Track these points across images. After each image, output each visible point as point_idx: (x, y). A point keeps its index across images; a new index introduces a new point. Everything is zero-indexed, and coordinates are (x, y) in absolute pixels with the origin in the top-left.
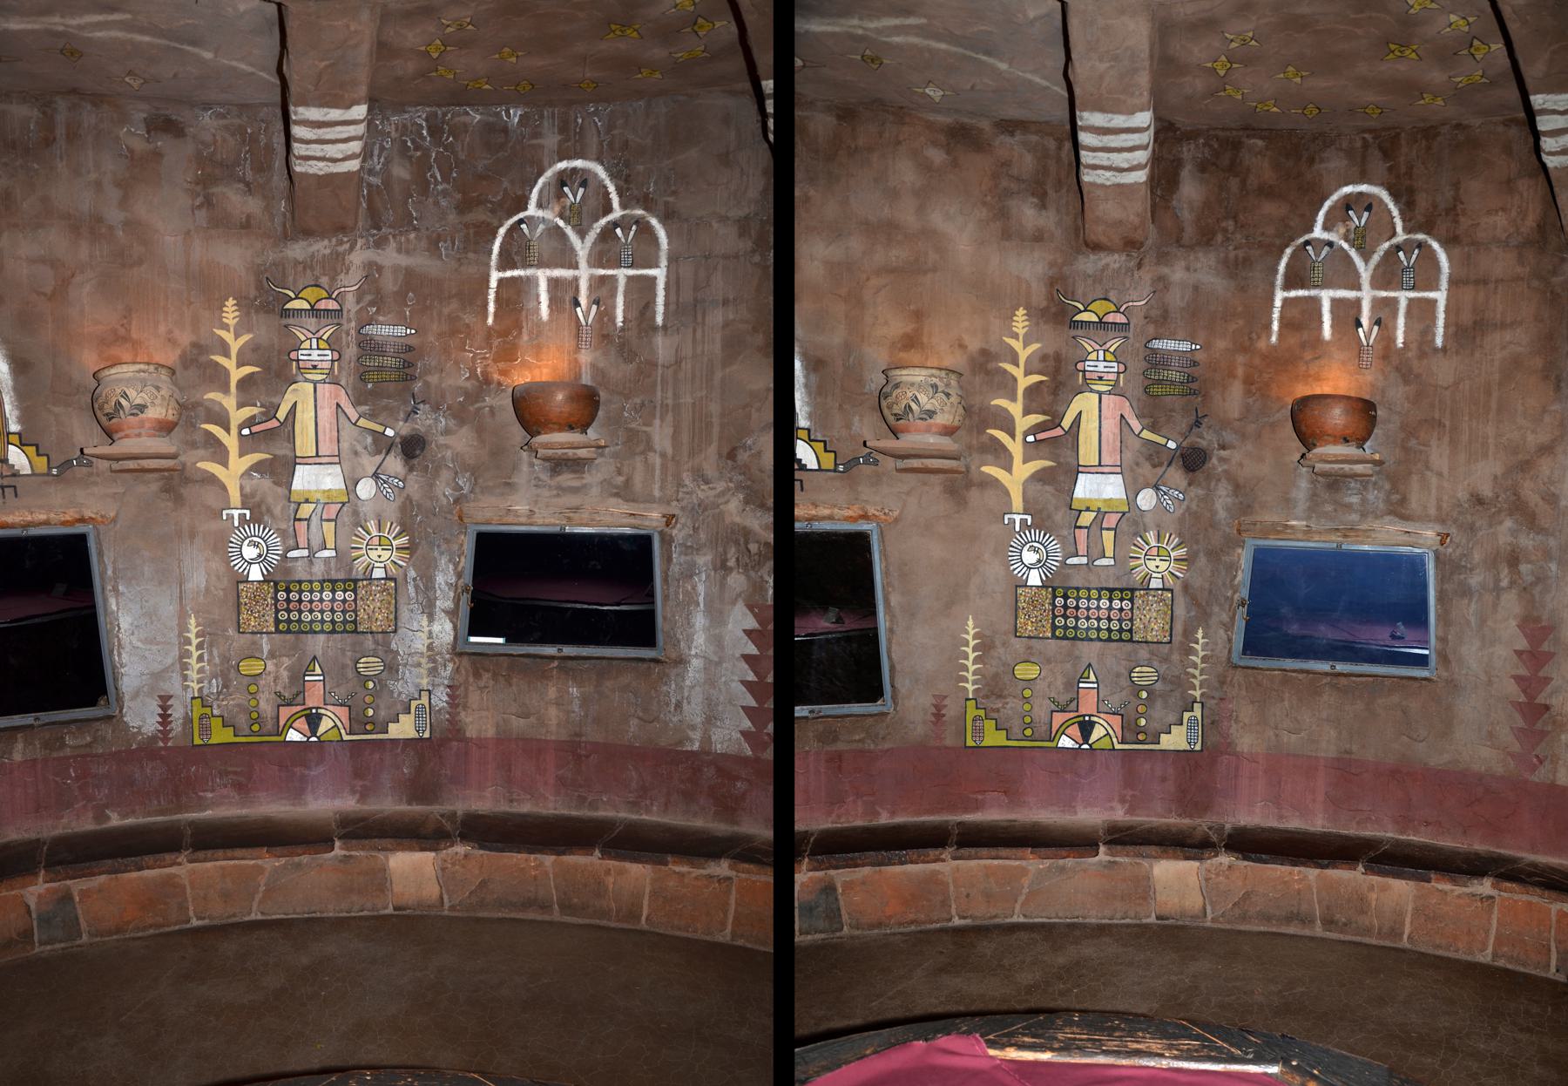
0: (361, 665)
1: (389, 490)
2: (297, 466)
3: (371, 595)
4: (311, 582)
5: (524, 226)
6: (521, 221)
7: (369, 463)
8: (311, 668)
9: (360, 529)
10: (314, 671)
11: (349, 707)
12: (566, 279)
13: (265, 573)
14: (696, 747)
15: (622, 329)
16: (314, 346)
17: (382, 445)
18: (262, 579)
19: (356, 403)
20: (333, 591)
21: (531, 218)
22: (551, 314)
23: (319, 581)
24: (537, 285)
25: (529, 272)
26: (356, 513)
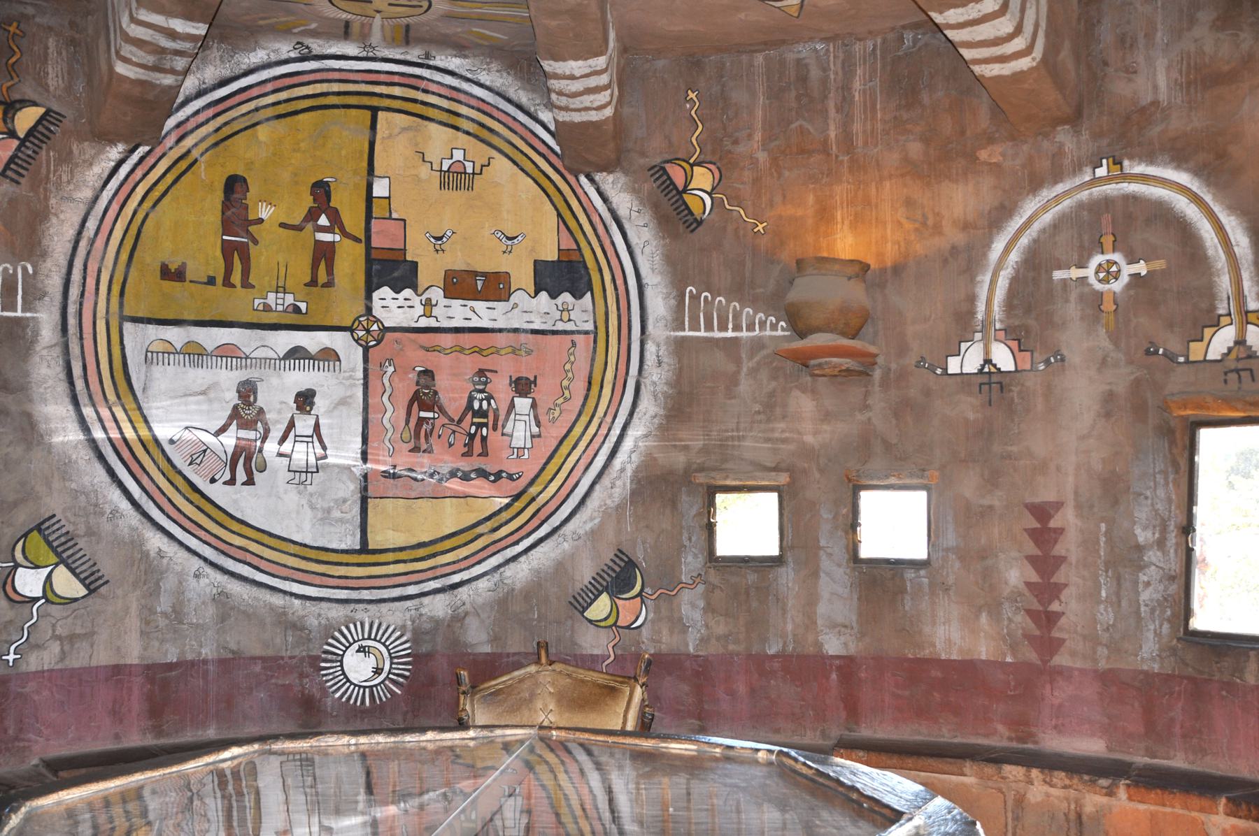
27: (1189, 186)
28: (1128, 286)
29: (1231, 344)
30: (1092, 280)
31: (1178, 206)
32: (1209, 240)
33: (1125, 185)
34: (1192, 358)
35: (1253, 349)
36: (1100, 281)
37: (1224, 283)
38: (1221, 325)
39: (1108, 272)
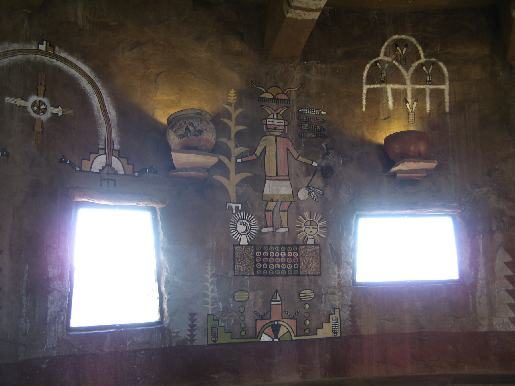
0: (302, 295)
1: (315, 196)
2: (267, 181)
3: (307, 254)
4: (274, 246)
5: (378, 64)
6: (377, 62)
7: (305, 181)
8: (274, 297)
9: (300, 217)
10: (276, 298)
11: (296, 319)
12: (400, 90)
13: (249, 240)
14: (485, 329)
15: (430, 114)
16: (275, 117)
17: (310, 171)
18: (248, 244)
19: (297, 149)
20: (286, 252)
21: (381, 61)
22: (394, 106)
23: (278, 246)
24: (386, 92)
25: (382, 86)
26: (298, 208)
27: (89, 74)
28: (50, 119)
29: (104, 165)
30: (30, 110)
31: (82, 83)
32: (96, 107)
33: (55, 60)
34: (83, 169)
35: (116, 170)
36: (34, 111)
37: (103, 131)
38: (100, 154)
39: (39, 108)
